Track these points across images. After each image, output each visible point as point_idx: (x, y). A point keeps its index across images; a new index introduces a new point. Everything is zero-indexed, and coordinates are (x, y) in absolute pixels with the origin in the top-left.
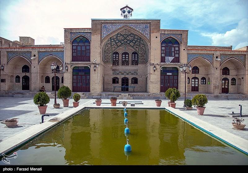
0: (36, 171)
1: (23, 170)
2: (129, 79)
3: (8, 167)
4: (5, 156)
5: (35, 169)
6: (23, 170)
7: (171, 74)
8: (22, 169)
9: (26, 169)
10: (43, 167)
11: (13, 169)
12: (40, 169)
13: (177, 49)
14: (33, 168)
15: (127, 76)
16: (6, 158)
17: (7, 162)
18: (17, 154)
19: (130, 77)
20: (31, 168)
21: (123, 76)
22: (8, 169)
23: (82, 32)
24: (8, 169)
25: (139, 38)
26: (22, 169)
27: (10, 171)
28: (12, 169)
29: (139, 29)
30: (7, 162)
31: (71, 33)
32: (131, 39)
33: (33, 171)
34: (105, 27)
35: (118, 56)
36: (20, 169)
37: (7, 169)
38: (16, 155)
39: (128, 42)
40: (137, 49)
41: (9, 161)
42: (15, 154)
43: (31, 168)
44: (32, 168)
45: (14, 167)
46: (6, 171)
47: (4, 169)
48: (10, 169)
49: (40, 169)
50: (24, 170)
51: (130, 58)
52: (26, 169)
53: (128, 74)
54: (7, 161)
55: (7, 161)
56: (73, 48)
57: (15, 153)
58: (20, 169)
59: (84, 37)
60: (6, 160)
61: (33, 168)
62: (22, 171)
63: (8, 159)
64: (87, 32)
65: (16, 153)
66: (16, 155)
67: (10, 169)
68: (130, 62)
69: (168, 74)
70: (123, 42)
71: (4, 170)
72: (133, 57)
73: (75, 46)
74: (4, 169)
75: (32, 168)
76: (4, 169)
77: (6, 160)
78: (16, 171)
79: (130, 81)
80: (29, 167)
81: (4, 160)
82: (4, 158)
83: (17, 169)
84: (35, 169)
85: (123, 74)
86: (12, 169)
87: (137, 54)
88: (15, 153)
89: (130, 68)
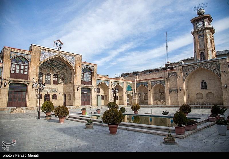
1: (21, 156)
2: (51, 95)
3: (7, 153)
4: (4, 143)
5: (32, 156)
6: (21, 156)
7: (86, 93)
8: (21, 156)
9: (24, 156)
10: (39, 153)
11: (12, 156)
12: (37, 156)
13: (90, 76)
14: (30, 154)
15: (49, 93)
17: (6, 149)
18: (15, 142)
19: (51, 94)
20: (28, 154)
21: (46, 93)
22: (8, 156)
23: (23, 53)
24: (8, 156)
25: (64, 65)
26: (21, 156)
28: (11, 156)
29: (68, 59)
30: (6, 149)
31: (11, 52)
32: (56, 64)
33: (31, 157)
34: (43, 53)
35: (50, 77)
36: (19, 156)
37: (7, 156)
38: (15, 143)
39: (53, 66)
40: (59, 73)
41: (8, 148)
43: (28, 154)
44: (29, 155)
45: (13, 153)
47: (4, 156)
48: (9, 156)
49: (37, 156)
50: (22, 156)
51: (52, 79)
52: (24, 156)
53: (49, 91)
54: (7, 148)
55: (7, 148)
56: (12, 66)
57: (13, 141)
58: (19, 156)
59: (24, 58)
60: (6, 147)
61: (30, 154)
62: (20, 158)
63: (7, 146)
64: (27, 54)
65: (15, 141)
66: (15, 143)
67: (9, 156)
68: (52, 82)
69: (84, 92)
70: (49, 66)
71: (3, 156)
72: (54, 78)
73: (14, 64)
74: (4, 156)
75: (29, 155)
76: (4, 156)
77: (6, 147)
79: (51, 97)
80: (27, 153)
81: (4, 147)
83: (16, 155)
84: (32, 156)
85: (45, 91)
86: (11, 156)
87: (57, 76)
88: (13, 141)
89: (51, 86)
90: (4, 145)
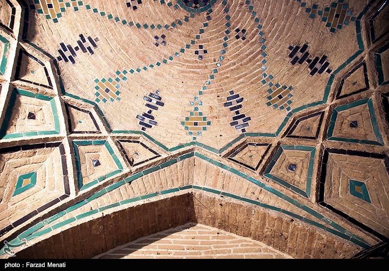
0: (57, 268)
1: (36, 266)
5: (54, 265)
6: (36, 266)
8: (35, 265)
9: (40, 265)
11: (21, 265)
14: (51, 263)
16: (10, 248)
17: (11, 254)
20: (48, 263)
22: (13, 265)
24: (13, 265)
26: (35, 265)
27: (15, 268)
28: (18, 265)
33: (52, 268)
36: (32, 265)
37: (11, 265)
42: (24, 242)
43: (48, 263)
44: (50, 263)
46: (9, 268)
47: (7, 265)
48: (16, 265)
50: (38, 266)
52: (40, 265)
58: (32, 265)
60: (10, 251)
61: (51, 263)
62: (34, 268)
67: (16, 265)
71: (6, 267)
74: (7, 265)
75: (50, 263)
76: (6, 265)
78: (25, 268)
81: (6, 251)
82: (7, 247)
83: (27, 265)
84: (54, 265)
86: (18, 265)
90: (7, 247)
